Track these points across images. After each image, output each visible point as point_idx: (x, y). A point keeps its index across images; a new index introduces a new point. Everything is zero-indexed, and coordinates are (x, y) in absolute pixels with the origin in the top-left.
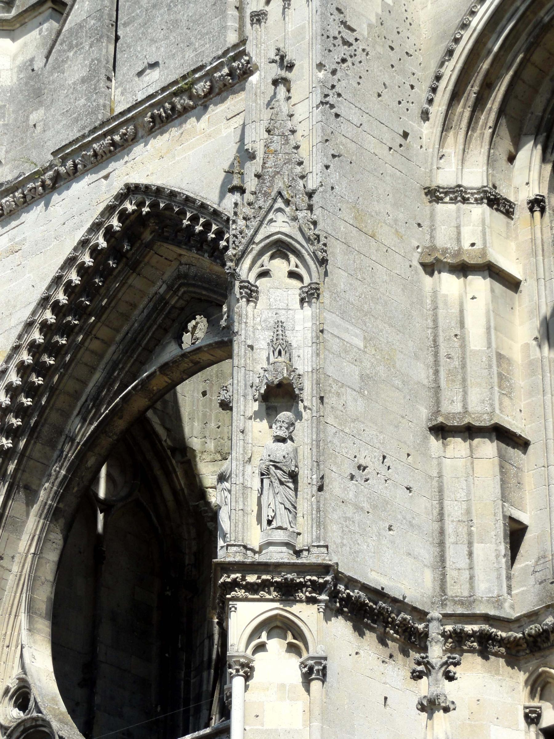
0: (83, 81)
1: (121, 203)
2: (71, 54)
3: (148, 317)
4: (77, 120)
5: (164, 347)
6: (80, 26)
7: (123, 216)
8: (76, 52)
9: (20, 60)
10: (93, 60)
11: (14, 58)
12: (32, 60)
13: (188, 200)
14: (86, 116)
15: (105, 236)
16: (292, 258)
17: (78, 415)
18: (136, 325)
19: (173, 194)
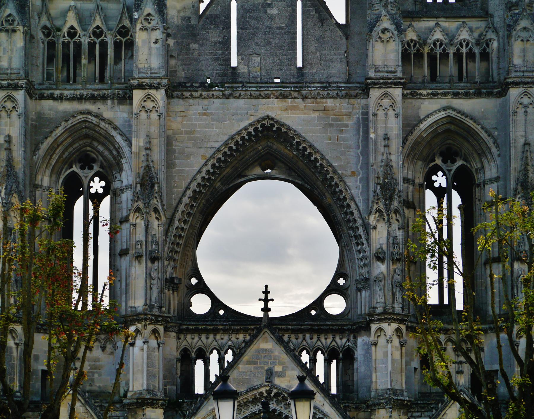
0: (220, 43)
1: (263, 120)
2: (212, 27)
3: (253, 156)
4: (217, 59)
5: (254, 167)
6: (216, 17)
7: (263, 125)
8: (214, 27)
9: (182, 14)
10: (224, 36)
11: (179, 11)
12: (189, 18)
13: (298, 135)
14: (223, 60)
15: (254, 129)
16: (398, 215)
17: (219, 182)
18: (247, 157)
19: (290, 129)
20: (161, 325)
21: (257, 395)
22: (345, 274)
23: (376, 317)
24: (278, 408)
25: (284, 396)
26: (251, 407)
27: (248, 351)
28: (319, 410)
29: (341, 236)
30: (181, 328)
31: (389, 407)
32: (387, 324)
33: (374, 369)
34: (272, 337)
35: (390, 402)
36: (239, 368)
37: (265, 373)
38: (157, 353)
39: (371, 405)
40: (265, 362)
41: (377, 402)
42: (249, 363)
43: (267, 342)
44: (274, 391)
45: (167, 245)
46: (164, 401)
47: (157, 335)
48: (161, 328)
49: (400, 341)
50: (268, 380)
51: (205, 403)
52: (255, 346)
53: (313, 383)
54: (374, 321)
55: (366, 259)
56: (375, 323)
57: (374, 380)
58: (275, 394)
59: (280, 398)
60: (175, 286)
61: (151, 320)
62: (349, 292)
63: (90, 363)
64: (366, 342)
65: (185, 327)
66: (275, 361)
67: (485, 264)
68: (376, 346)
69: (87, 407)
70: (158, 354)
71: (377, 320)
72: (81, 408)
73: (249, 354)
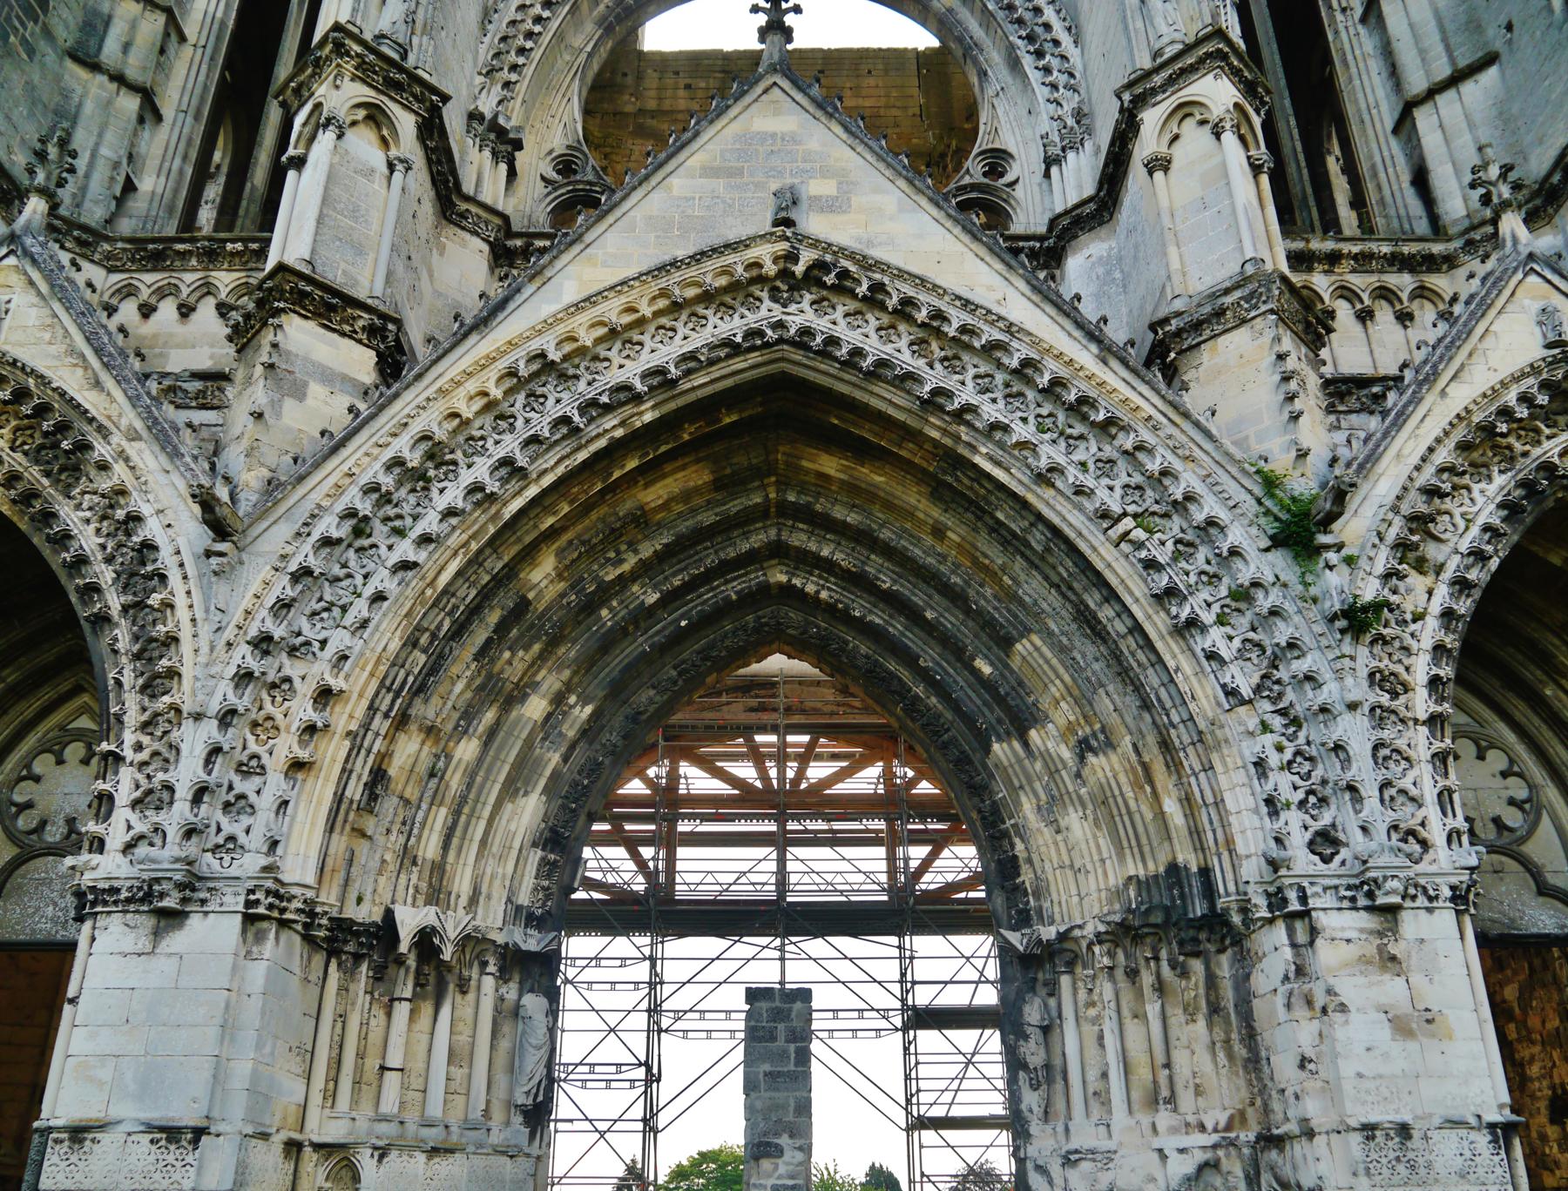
20: (406, 107)
21: (740, 269)
22: (1004, 151)
23: (1158, 80)
24: (821, 324)
25: (844, 274)
26: (713, 320)
27: (704, 137)
28: (989, 312)
29: (983, 74)
30: (510, 243)
31: (1264, 308)
32: (1211, 76)
33: (1169, 236)
34: (799, 97)
35: (1269, 290)
36: (670, 189)
37: (771, 201)
38: (378, 185)
39: (1179, 333)
40: (773, 169)
41: (1207, 309)
42: (709, 171)
43: (777, 113)
44: (807, 256)
45: (486, 40)
46: (385, 317)
47: (385, 132)
48: (406, 122)
49: (1249, 158)
50: (783, 214)
51: (529, 290)
52: (732, 126)
53: (957, 230)
54: (1153, 91)
55: (1072, 75)
56: (1159, 98)
57: (1175, 265)
58: (809, 269)
59: (830, 279)
60: (502, 148)
61: (362, 65)
62: (1019, 192)
63: (215, 350)
64: (1101, 258)
65: (519, 243)
66: (808, 166)
67: (1404, 123)
68: (1166, 170)
69: (57, 307)
70: (384, 191)
71: (1163, 88)
72: (34, 312)
73: (709, 147)
